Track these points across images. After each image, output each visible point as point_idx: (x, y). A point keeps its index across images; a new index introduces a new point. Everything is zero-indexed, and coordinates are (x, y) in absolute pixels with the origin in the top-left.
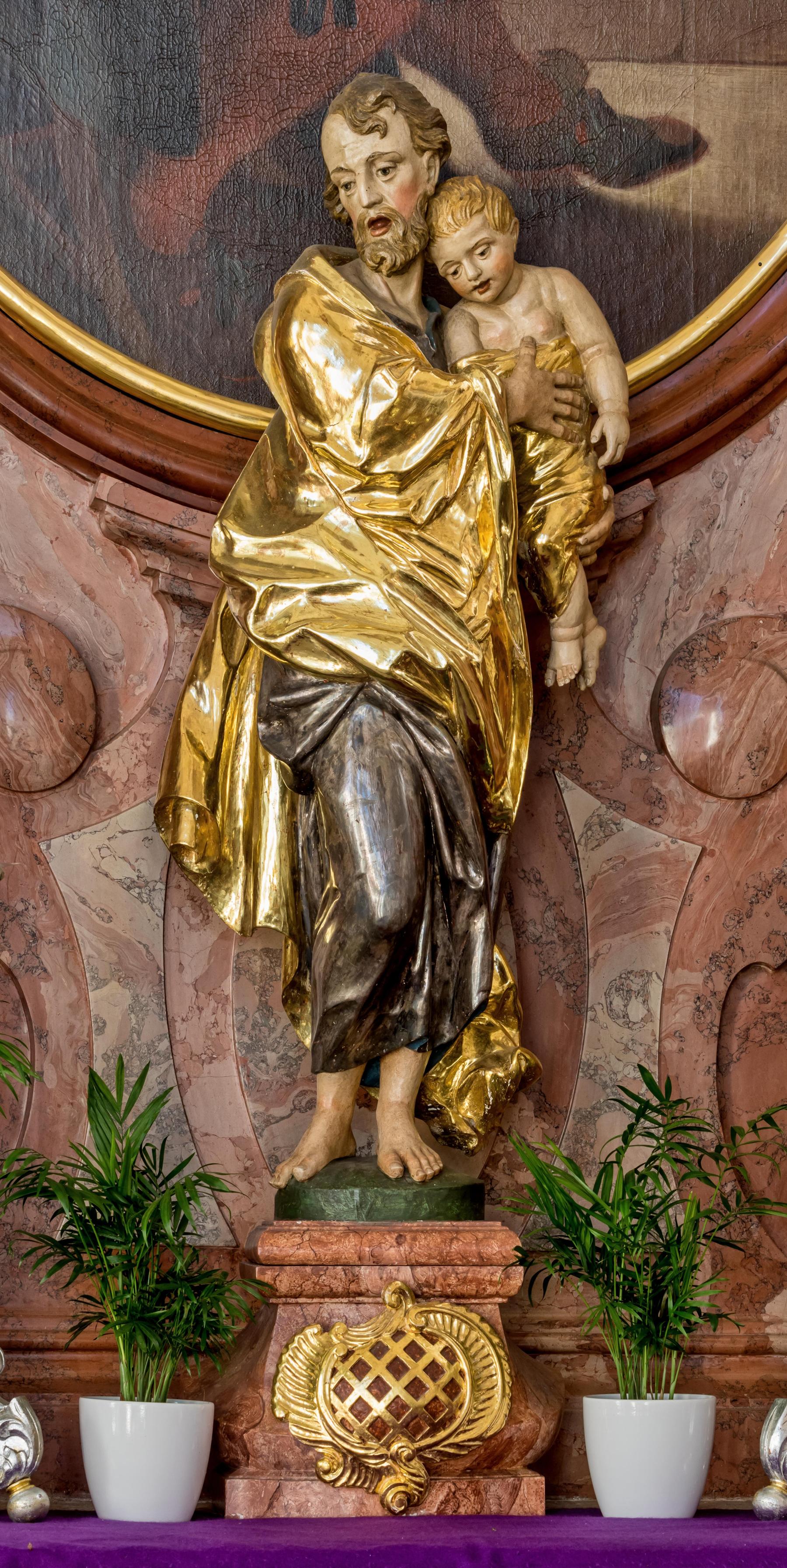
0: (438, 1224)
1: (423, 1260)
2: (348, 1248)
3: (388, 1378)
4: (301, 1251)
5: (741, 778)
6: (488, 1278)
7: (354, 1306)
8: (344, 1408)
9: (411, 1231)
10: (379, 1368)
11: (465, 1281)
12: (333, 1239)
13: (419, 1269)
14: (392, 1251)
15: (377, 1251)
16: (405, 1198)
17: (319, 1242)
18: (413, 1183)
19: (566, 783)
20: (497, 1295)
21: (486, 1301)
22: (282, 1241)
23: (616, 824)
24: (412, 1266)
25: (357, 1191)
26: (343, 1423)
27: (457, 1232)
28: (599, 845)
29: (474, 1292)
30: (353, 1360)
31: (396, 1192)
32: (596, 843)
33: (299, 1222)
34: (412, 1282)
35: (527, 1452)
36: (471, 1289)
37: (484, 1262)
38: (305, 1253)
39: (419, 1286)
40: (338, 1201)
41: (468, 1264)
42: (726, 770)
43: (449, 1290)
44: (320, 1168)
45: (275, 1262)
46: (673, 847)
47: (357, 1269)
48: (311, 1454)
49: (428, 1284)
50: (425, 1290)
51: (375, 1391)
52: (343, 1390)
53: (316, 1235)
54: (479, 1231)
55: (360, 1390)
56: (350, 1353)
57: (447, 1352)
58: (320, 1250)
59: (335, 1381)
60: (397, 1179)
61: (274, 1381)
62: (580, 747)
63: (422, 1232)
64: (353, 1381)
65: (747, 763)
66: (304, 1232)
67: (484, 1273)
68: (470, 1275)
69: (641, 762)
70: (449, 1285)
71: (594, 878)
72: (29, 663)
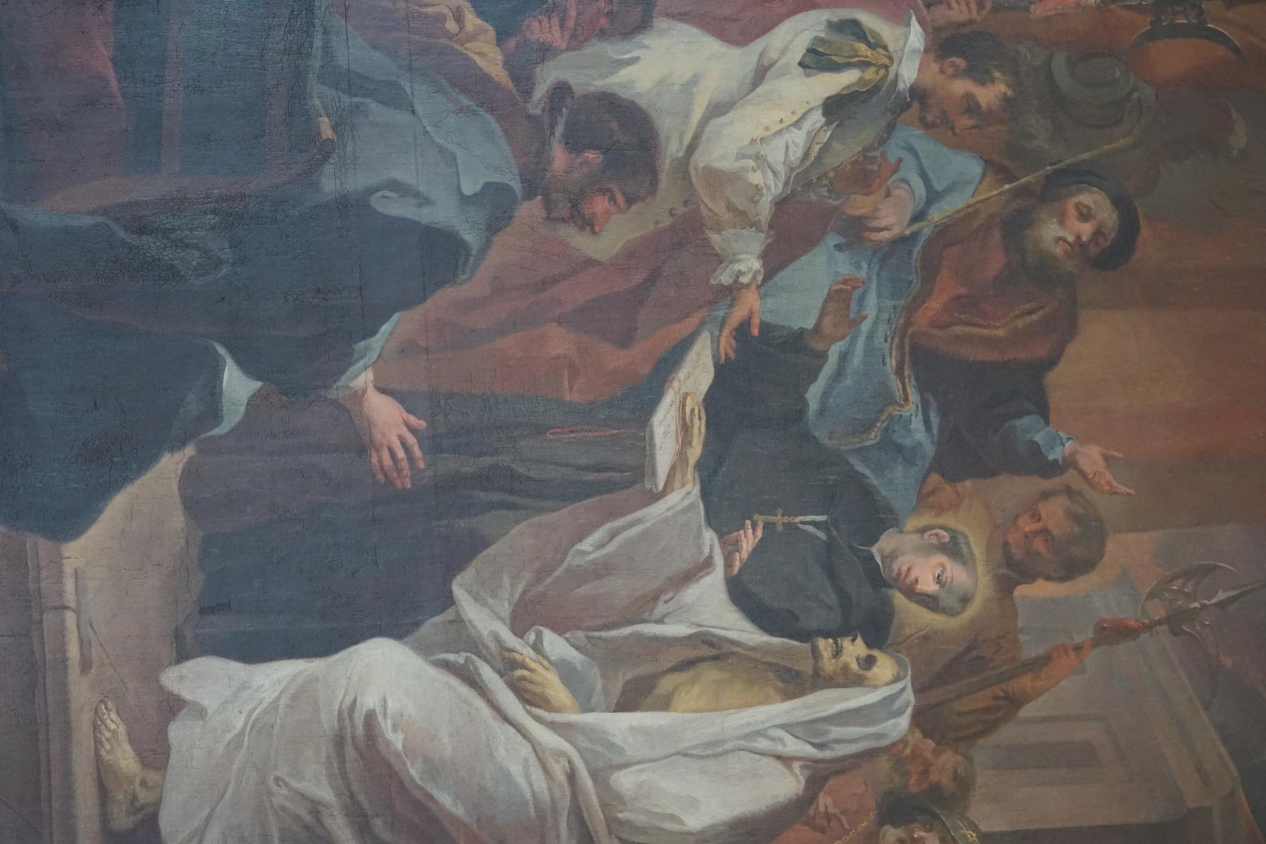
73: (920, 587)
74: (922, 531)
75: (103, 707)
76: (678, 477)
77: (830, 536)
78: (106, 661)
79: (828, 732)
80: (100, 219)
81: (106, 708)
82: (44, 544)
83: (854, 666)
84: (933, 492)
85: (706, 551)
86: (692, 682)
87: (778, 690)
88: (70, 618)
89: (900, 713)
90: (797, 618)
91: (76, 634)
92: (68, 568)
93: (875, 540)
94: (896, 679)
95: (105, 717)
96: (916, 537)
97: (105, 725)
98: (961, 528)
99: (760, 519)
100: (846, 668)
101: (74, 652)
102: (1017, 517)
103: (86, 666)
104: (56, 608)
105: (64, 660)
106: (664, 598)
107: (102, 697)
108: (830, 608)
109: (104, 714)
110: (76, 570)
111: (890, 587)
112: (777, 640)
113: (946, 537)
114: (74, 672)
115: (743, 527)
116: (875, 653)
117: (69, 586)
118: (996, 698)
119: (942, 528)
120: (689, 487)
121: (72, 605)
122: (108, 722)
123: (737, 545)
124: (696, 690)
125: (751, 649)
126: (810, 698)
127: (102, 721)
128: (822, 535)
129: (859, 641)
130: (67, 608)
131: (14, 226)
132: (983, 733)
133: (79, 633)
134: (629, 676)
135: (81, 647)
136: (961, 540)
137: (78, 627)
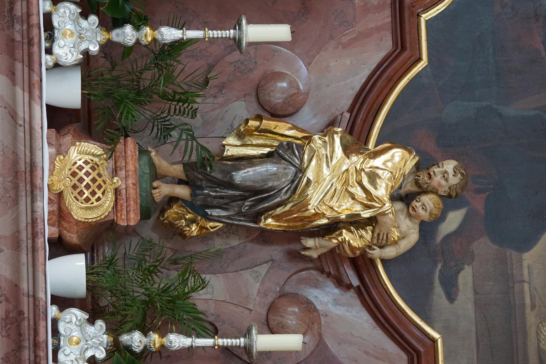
0: (139, 198)
1: (128, 192)
2: (131, 167)
3: (91, 177)
4: (129, 151)
5: (274, 320)
6: (123, 213)
7: (112, 171)
8: (80, 163)
9: (136, 189)
10: (94, 174)
11: (121, 206)
12: (133, 162)
13: (125, 190)
14: (130, 182)
15: (131, 176)
16: (146, 187)
17: (132, 158)
18: (151, 191)
19: (269, 264)
20: (117, 217)
21: (115, 214)
22: (132, 145)
23: (258, 281)
24: (126, 188)
25: (148, 171)
26: (76, 163)
27: (137, 204)
28: (251, 275)
29: (118, 209)
30: (96, 166)
31: (149, 184)
32: (252, 275)
33: (138, 152)
34: (121, 188)
35: (66, 230)
36: (119, 208)
37: (128, 212)
38: (129, 153)
39: (120, 191)
40: (145, 165)
41: (127, 207)
42: (276, 315)
43: (118, 201)
44: (154, 161)
45: (125, 143)
46: (252, 300)
47: (124, 170)
48: (65, 154)
49: (120, 193)
50: (118, 193)
51: (87, 173)
52: (86, 162)
53: (134, 157)
54: (137, 211)
55: (87, 168)
56: (98, 166)
57: (99, 199)
58: (130, 157)
59: (89, 161)
60: (152, 185)
61: (88, 142)
62: (280, 269)
63: (136, 192)
64: (89, 166)
65: (279, 322)
66: (135, 153)
67: (125, 212)
68: (123, 207)
69: (277, 289)
70: (120, 201)
71: (242, 275)
72: (294, 94)
75: (541, 325)
78: (542, 305)
80: (538, 112)
81: (542, 326)
82: (514, 253)
88: (526, 286)
91: (529, 293)
92: (525, 264)
95: (542, 329)
97: (542, 333)
101: (528, 301)
103: (533, 307)
104: (521, 281)
105: (524, 304)
107: (540, 321)
109: (541, 328)
110: (528, 265)
114: (528, 310)
117: (526, 272)
121: (527, 280)
122: (543, 332)
127: (540, 331)
130: (525, 281)
131: (500, 115)
133: (530, 293)
135: (531, 299)
137: (530, 290)
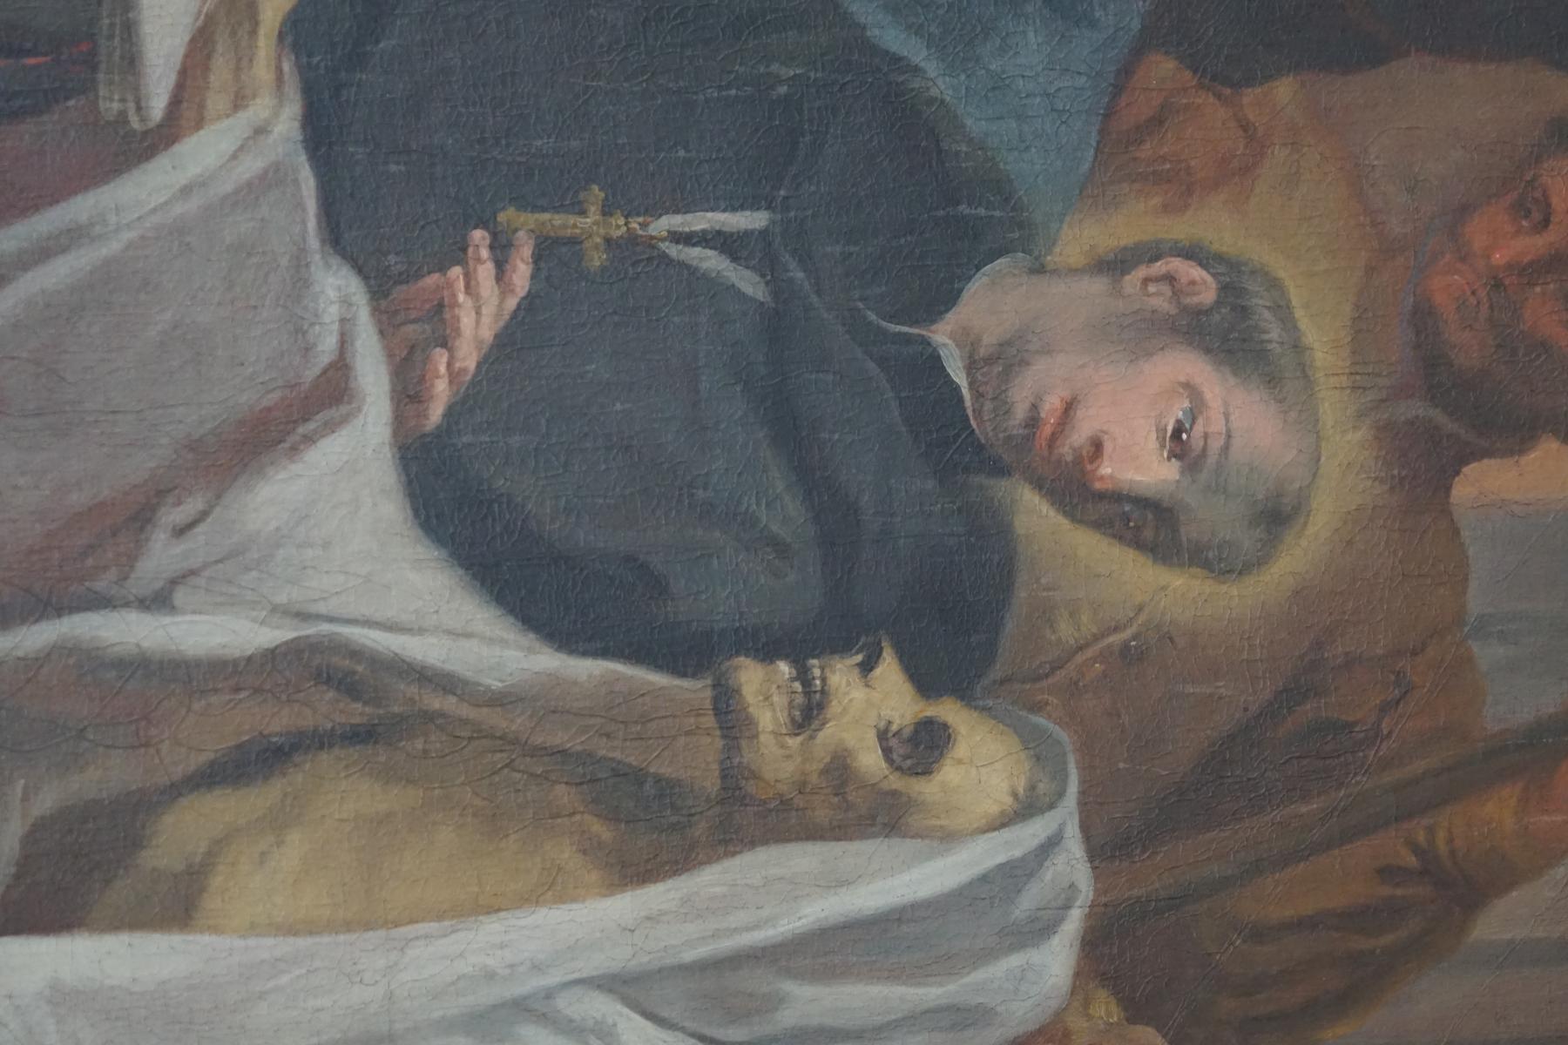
73: (1109, 470)
74: (1115, 265)
76: (221, 70)
77: (780, 288)
79: (774, 1002)
83: (870, 761)
84: (1157, 121)
85: (327, 345)
86: (277, 823)
87: (590, 849)
89: (1039, 930)
90: (658, 586)
93: (942, 299)
94: (1026, 808)
96: (1097, 286)
98: (1258, 252)
99: (524, 225)
100: (840, 769)
102: (1464, 211)
106: (173, 515)
108: (781, 548)
111: (1001, 470)
112: (586, 669)
113: (1203, 285)
115: (459, 253)
116: (949, 711)
118: (1387, 873)
119: (1191, 253)
120: (260, 108)
123: (439, 312)
124: (295, 847)
125: (500, 700)
126: (709, 880)
128: (749, 283)
129: (889, 669)
132: (1344, 1002)
134: (47, 801)
136: (1260, 303)
